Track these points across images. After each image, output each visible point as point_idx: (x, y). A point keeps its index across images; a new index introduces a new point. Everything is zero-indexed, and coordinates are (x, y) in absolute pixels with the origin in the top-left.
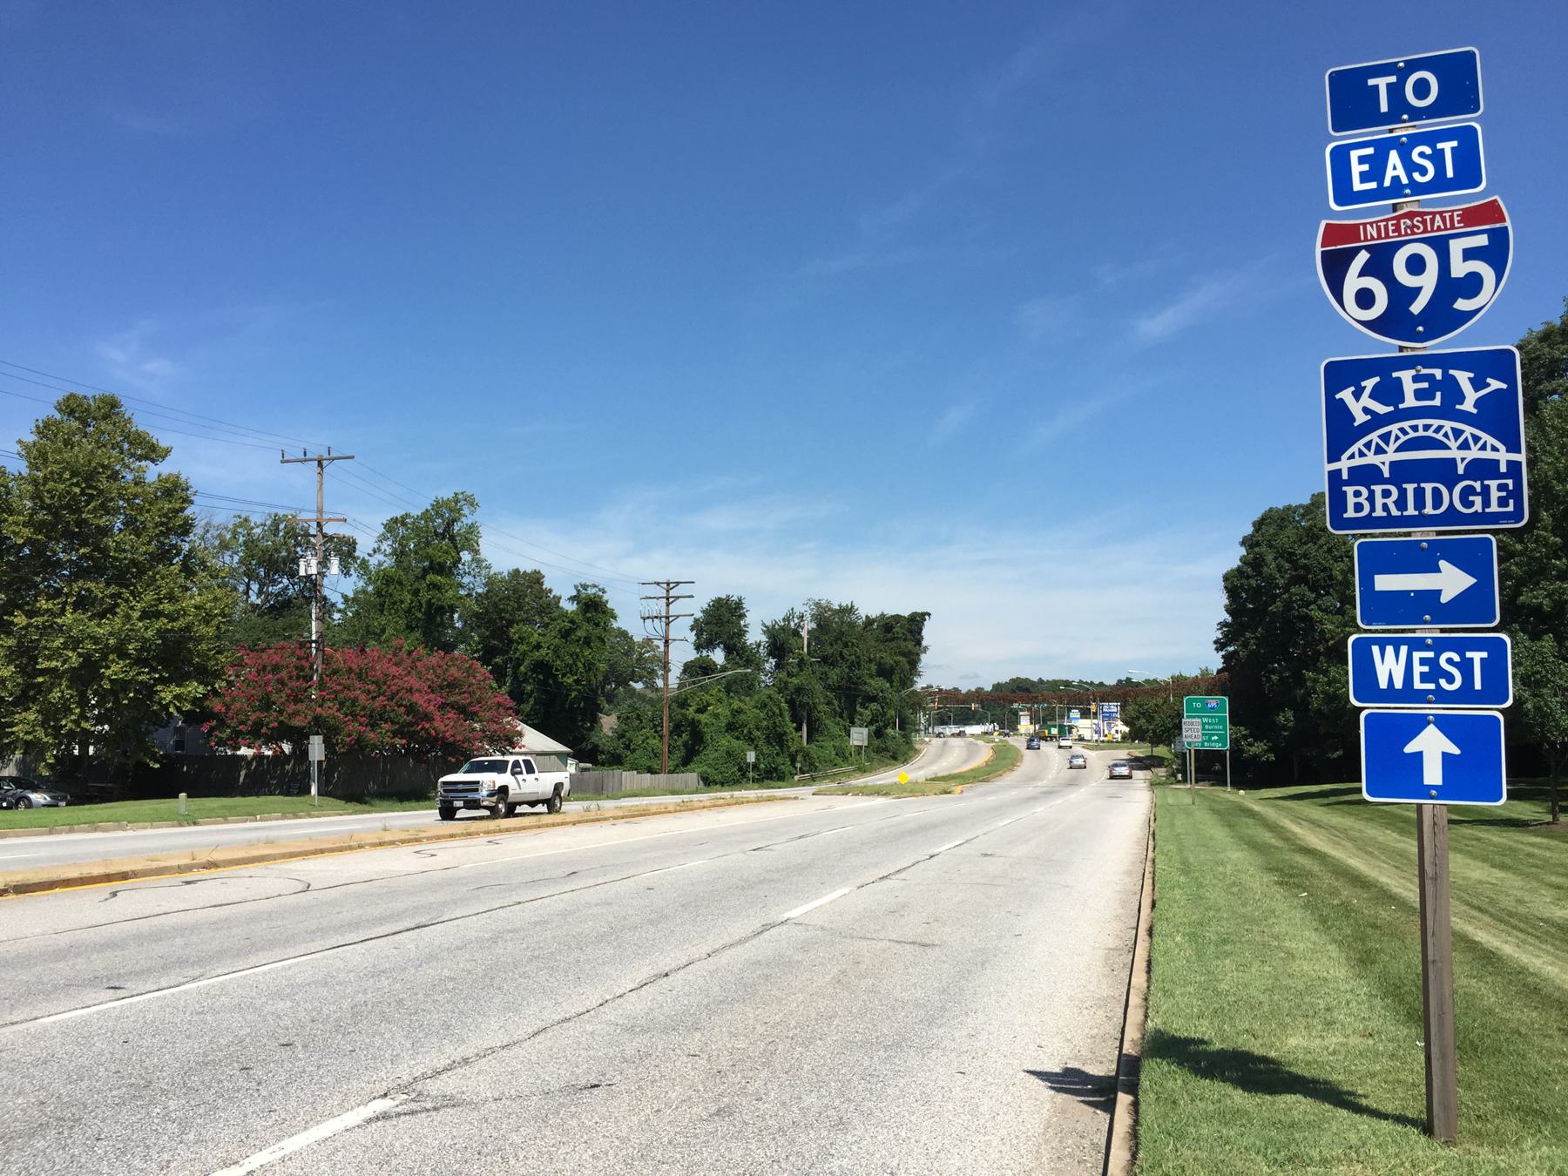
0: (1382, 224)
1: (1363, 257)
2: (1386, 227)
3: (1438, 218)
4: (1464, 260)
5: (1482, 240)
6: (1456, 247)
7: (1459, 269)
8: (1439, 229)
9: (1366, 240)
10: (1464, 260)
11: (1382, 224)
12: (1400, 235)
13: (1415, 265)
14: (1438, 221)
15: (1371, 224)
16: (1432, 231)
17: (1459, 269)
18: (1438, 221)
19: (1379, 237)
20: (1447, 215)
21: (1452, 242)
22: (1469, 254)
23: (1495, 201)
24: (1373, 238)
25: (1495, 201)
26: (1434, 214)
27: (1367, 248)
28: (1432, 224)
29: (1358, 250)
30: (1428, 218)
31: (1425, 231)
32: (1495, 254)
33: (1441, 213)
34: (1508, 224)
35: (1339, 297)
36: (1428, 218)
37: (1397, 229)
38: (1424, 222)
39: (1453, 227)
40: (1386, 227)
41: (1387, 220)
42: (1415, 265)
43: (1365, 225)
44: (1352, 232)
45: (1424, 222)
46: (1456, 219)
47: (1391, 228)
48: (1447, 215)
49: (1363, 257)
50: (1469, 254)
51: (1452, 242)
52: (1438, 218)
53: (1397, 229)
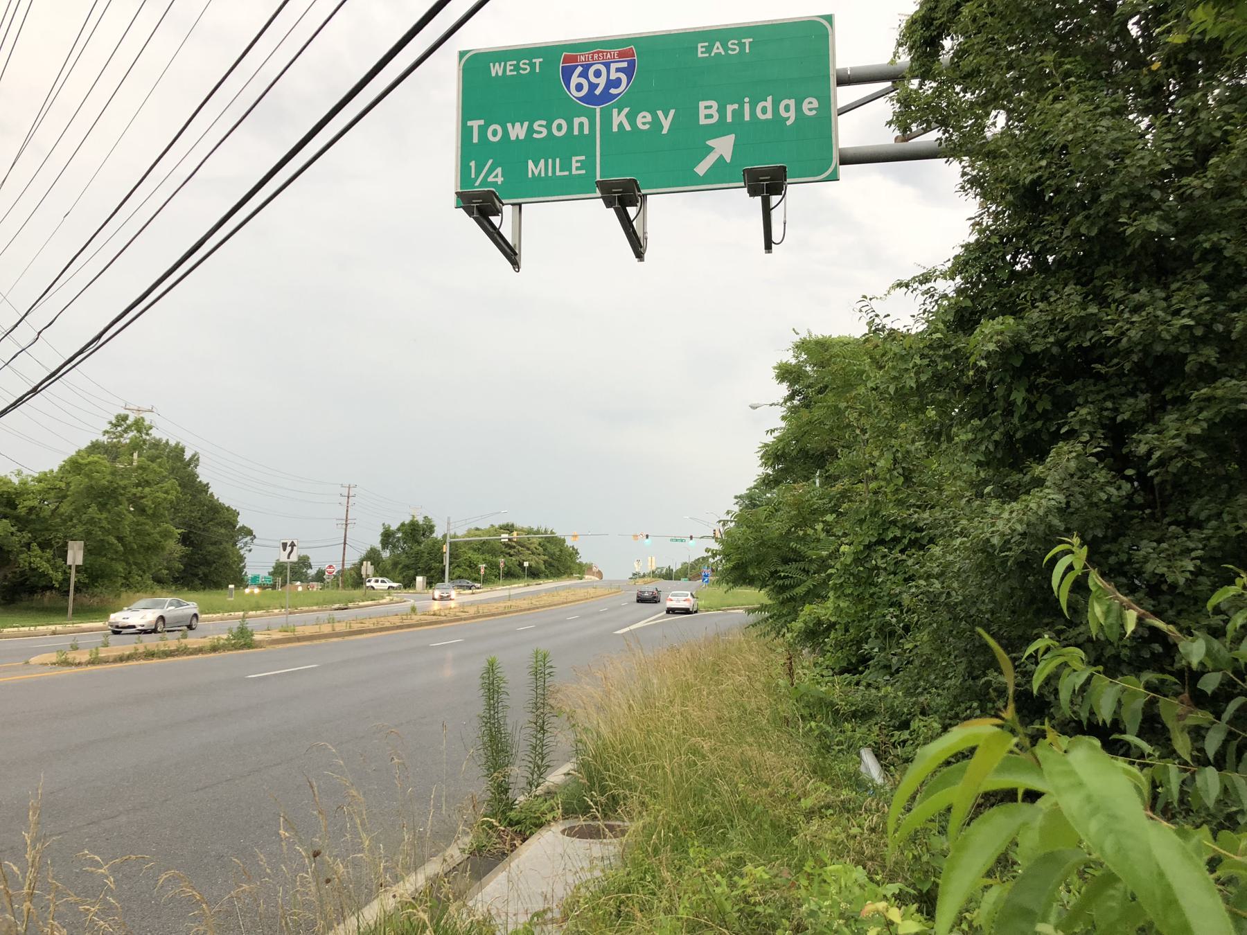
1: (580, 69)
5: (625, 65)
6: (613, 67)
7: (613, 76)
14: (609, 56)
18: (609, 56)
21: (612, 64)
22: (618, 70)
27: (582, 66)
29: (578, 66)
32: (629, 72)
35: (568, 88)
37: (593, 57)
38: (603, 56)
42: (598, 74)
44: (574, 59)
45: (603, 56)
49: (580, 69)
50: (618, 70)
51: (612, 64)
53: (593, 57)
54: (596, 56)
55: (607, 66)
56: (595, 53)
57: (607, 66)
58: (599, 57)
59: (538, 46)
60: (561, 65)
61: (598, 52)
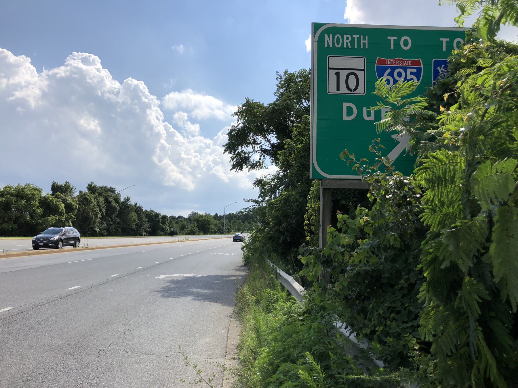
0: (392, 61)
2: (393, 62)
3: (405, 61)
4: (410, 75)
5: (415, 70)
6: (409, 71)
8: (405, 65)
9: (388, 64)
10: (410, 75)
11: (392, 61)
12: (396, 65)
13: (400, 75)
14: (405, 63)
15: (389, 60)
16: (404, 65)
17: (409, 77)
18: (405, 63)
19: (391, 64)
20: (408, 61)
22: (412, 73)
23: (419, 60)
24: (389, 64)
25: (419, 60)
26: (405, 60)
28: (404, 64)
30: (403, 61)
31: (402, 65)
33: (406, 61)
34: (422, 66)
36: (403, 61)
39: (409, 65)
40: (393, 62)
41: (393, 60)
43: (388, 60)
45: (402, 62)
46: (410, 63)
47: (394, 62)
48: (408, 61)
50: (412, 73)
52: (405, 61)
53: (396, 63)
54: (397, 63)
55: (405, 69)
56: (397, 60)
57: (405, 69)
58: (399, 63)
59: (134, 237)
60: (376, 65)
61: (399, 60)
